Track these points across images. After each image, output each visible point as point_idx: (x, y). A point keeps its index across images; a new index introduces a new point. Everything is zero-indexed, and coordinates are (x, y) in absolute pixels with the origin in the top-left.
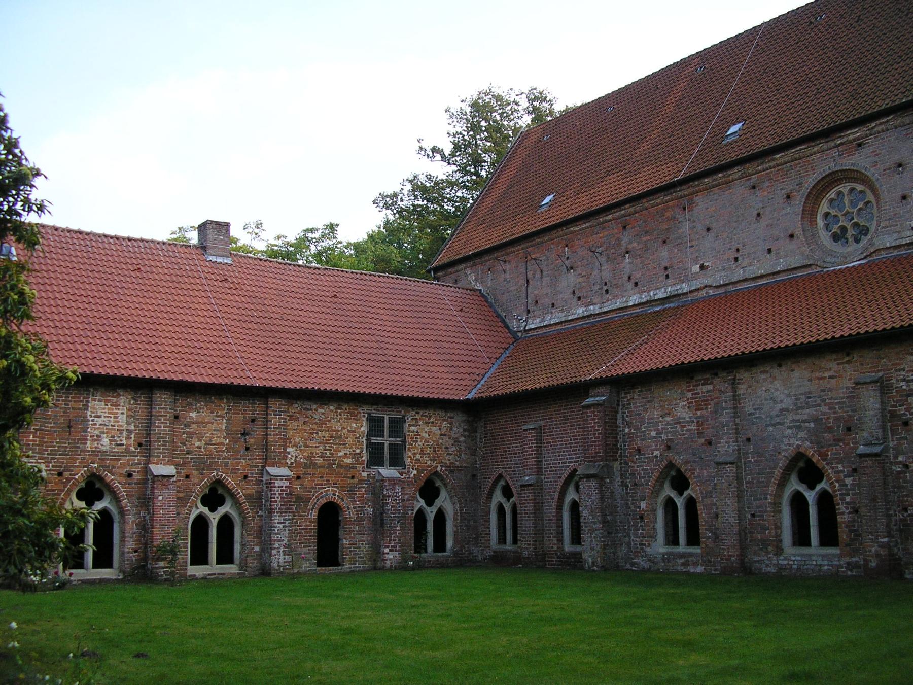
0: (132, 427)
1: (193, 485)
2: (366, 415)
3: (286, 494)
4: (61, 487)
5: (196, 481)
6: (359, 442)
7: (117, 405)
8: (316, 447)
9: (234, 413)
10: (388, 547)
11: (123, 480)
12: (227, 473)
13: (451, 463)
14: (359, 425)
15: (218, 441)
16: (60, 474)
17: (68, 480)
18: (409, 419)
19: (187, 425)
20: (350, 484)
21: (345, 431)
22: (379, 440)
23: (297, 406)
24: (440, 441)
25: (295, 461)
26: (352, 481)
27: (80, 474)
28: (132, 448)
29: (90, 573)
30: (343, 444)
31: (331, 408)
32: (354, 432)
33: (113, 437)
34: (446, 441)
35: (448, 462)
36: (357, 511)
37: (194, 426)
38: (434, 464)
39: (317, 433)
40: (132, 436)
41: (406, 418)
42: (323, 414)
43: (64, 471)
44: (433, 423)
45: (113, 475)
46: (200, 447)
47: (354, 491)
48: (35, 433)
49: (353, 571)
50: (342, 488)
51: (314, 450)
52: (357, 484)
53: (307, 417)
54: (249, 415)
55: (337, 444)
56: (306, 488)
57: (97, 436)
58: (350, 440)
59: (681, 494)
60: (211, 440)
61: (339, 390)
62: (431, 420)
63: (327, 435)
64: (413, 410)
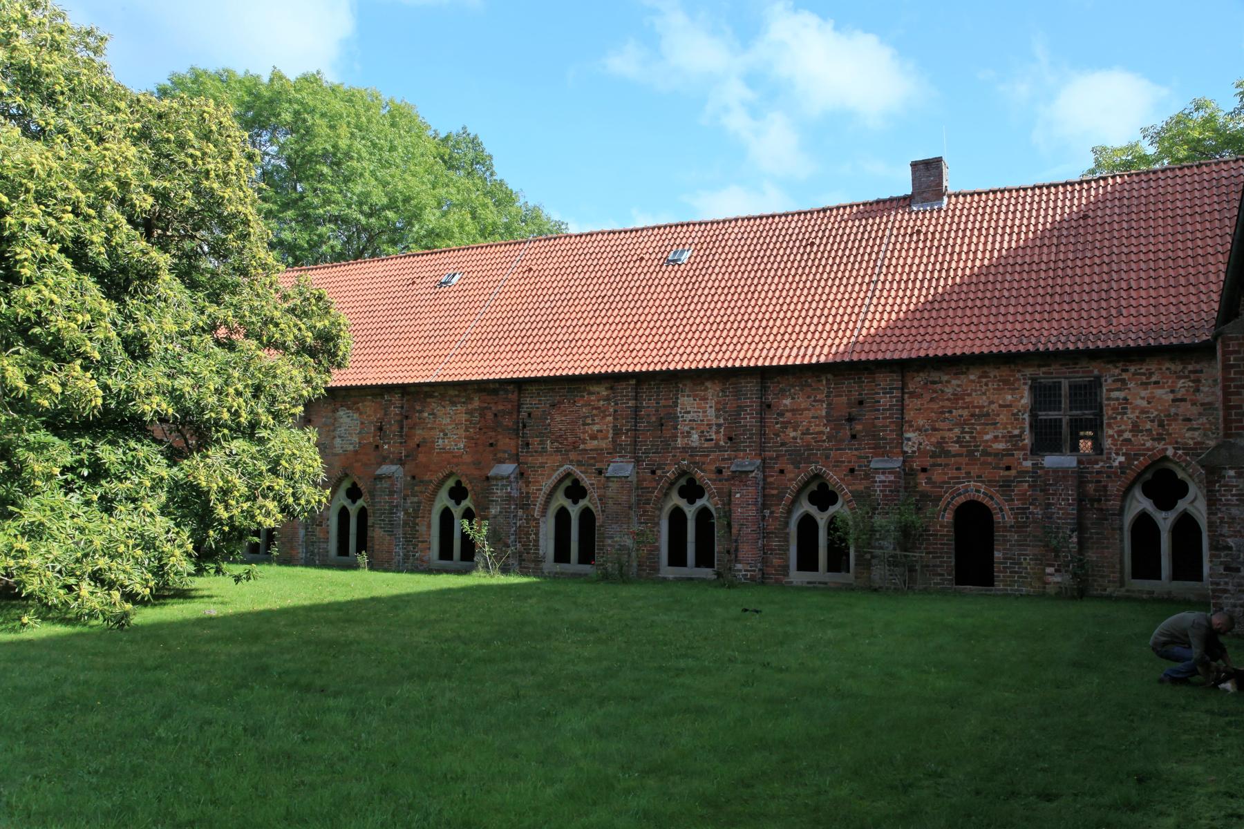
0: (722, 421)
1: (789, 480)
2: (1030, 382)
3: (890, 491)
4: (654, 484)
5: (792, 475)
6: (1017, 419)
7: (704, 399)
8: (950, 430)
9: (836, 396)
10: (1052, 566)
11: (713, 476)
12: (828, 467)
13: (1195, 443)
14: (1018, 396)
15: (817, 429)
16: (653, 472)
17: (661, 478)
18: (1108, 383)
19: (781, 414)
20: (1003, 476)
21: (993, 406)
22: (1053, 415)
23: (920, 379)
24: (1173, 411)
25: (919, 449)
26: (1007, 473)
27: (671, 472)
28: (722, 443)
29: (690, 570)
30: (992, 424)
31: (972, 377)
32: (1010, 406)
33: (702, 432)
34: (1186, 409)
35: (1191, 442)
36: (1015, 514)
37: (788, 415)
38: (1161, 446)
39: (950, 412)
40: (722, 430)
41: (1103, 379)
42: (959, 386)
43: (657, 469)
44: (1156, 383)
45: (702, 471)
46: (795, 438)
47: (1010, 486)
48: (627, 433)
49: (1009, 595)
50: (990, 483)
51: (947, 434)
52: (1015, 477)
53: (935, 391)
54: (855, 395)
55: (983, 424)
56: (935, 483)
57: (688, 432)
58: (1003, 418)
59: (458, 503)
60: (808, 429)
61: (931, 355)
62: (1154, 379)
63: (965, 413)
64: (1117, 367)
